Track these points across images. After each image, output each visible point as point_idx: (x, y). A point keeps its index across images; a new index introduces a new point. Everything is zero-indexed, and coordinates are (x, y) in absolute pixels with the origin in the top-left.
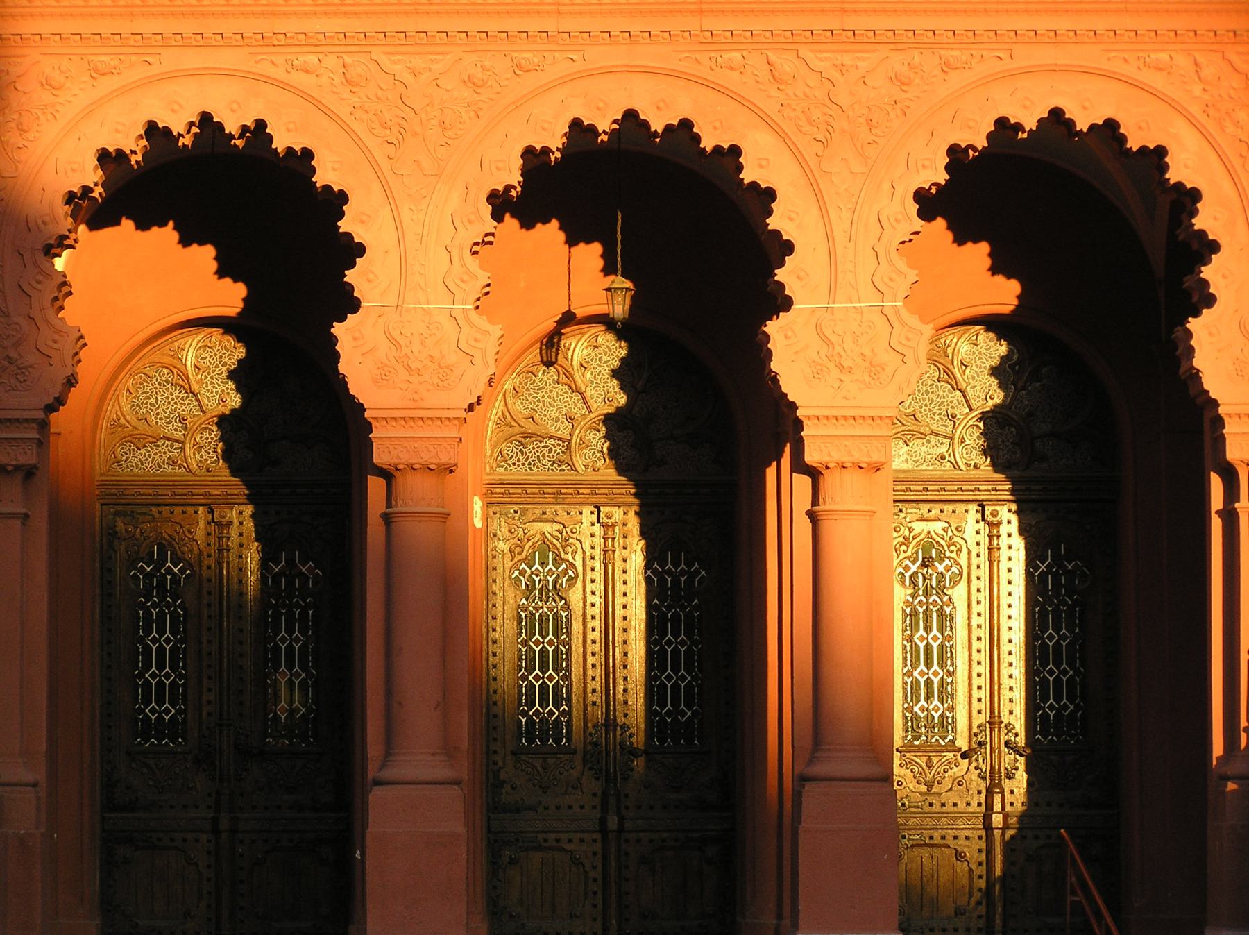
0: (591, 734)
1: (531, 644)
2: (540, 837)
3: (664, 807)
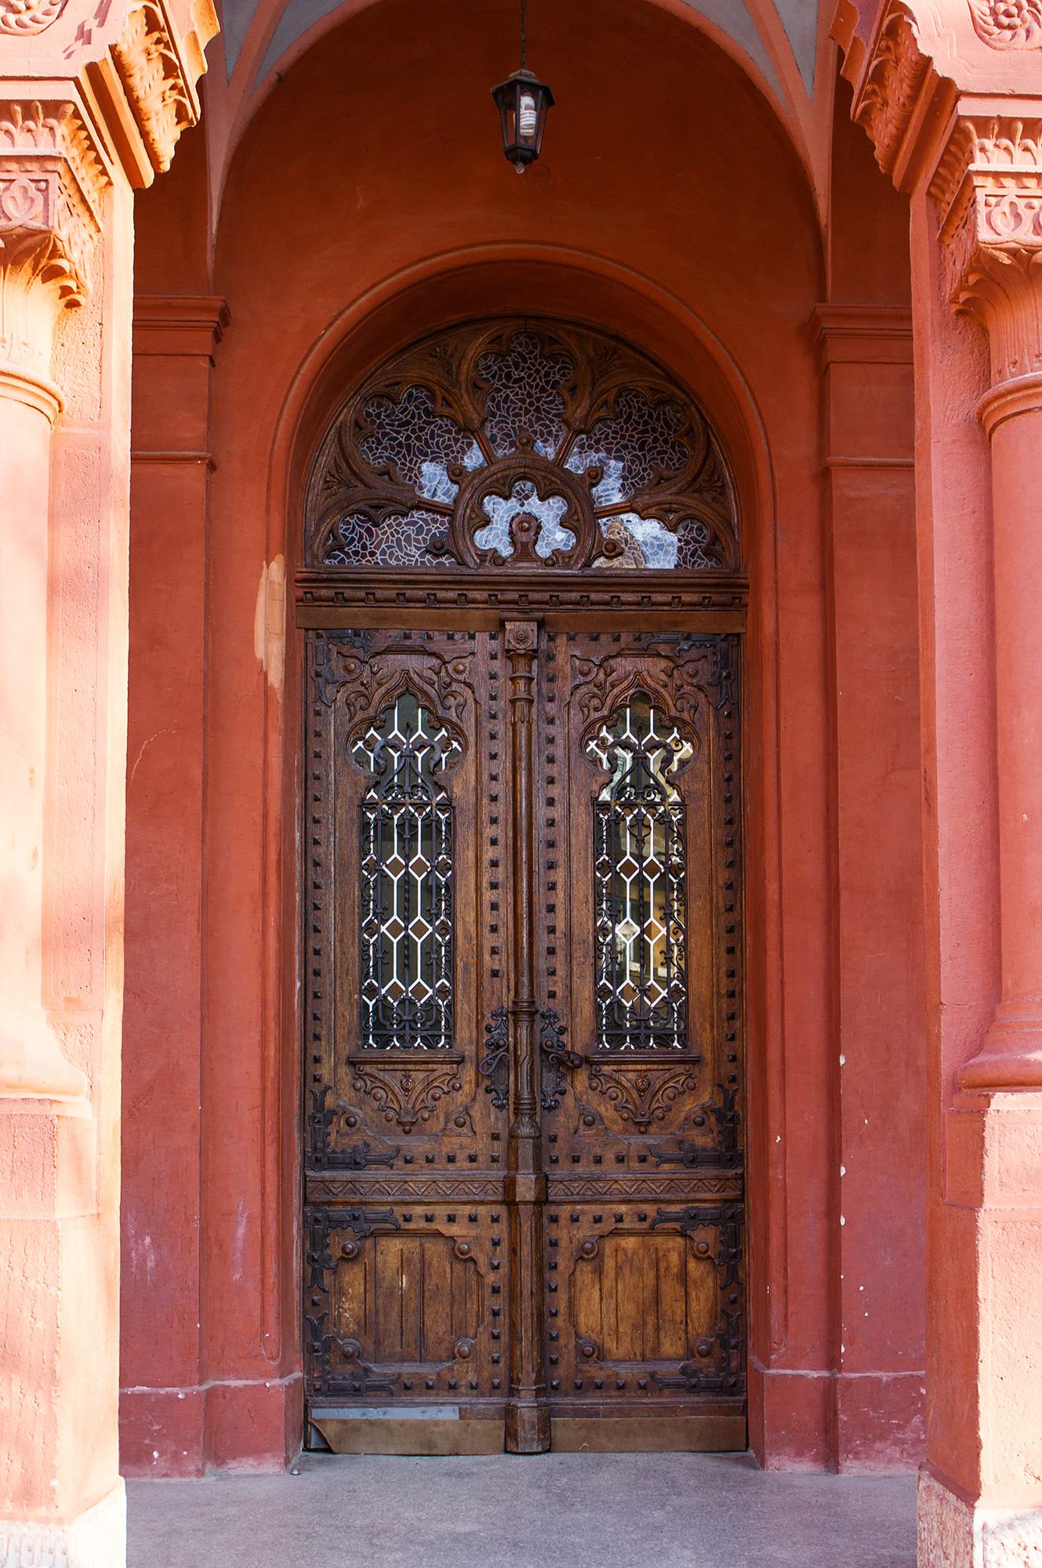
1: (384, 868)
2: (399, 1211)
3: (620, 1159)
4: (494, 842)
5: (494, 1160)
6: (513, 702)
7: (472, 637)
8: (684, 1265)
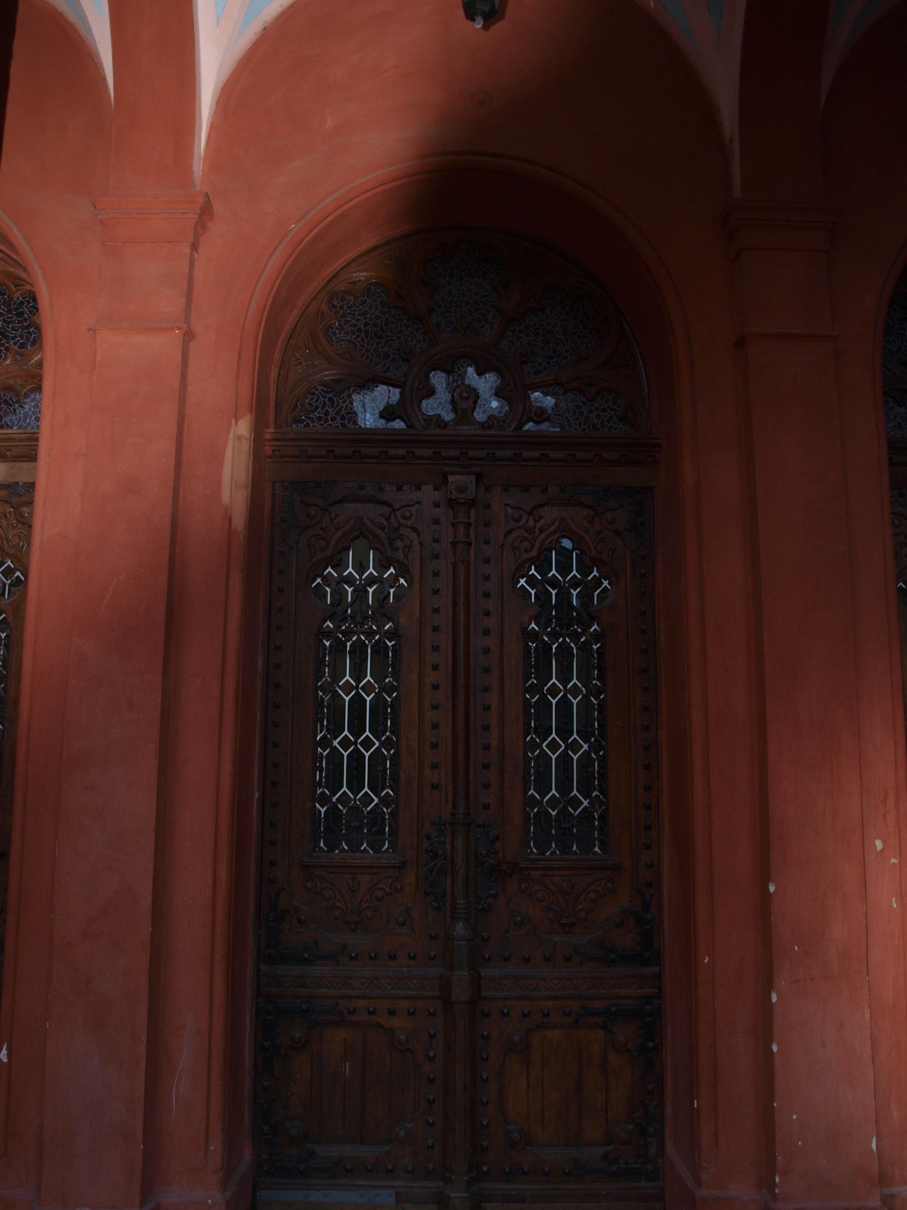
4: (435, 668)
6: (454, 544)
7: (418, 488)
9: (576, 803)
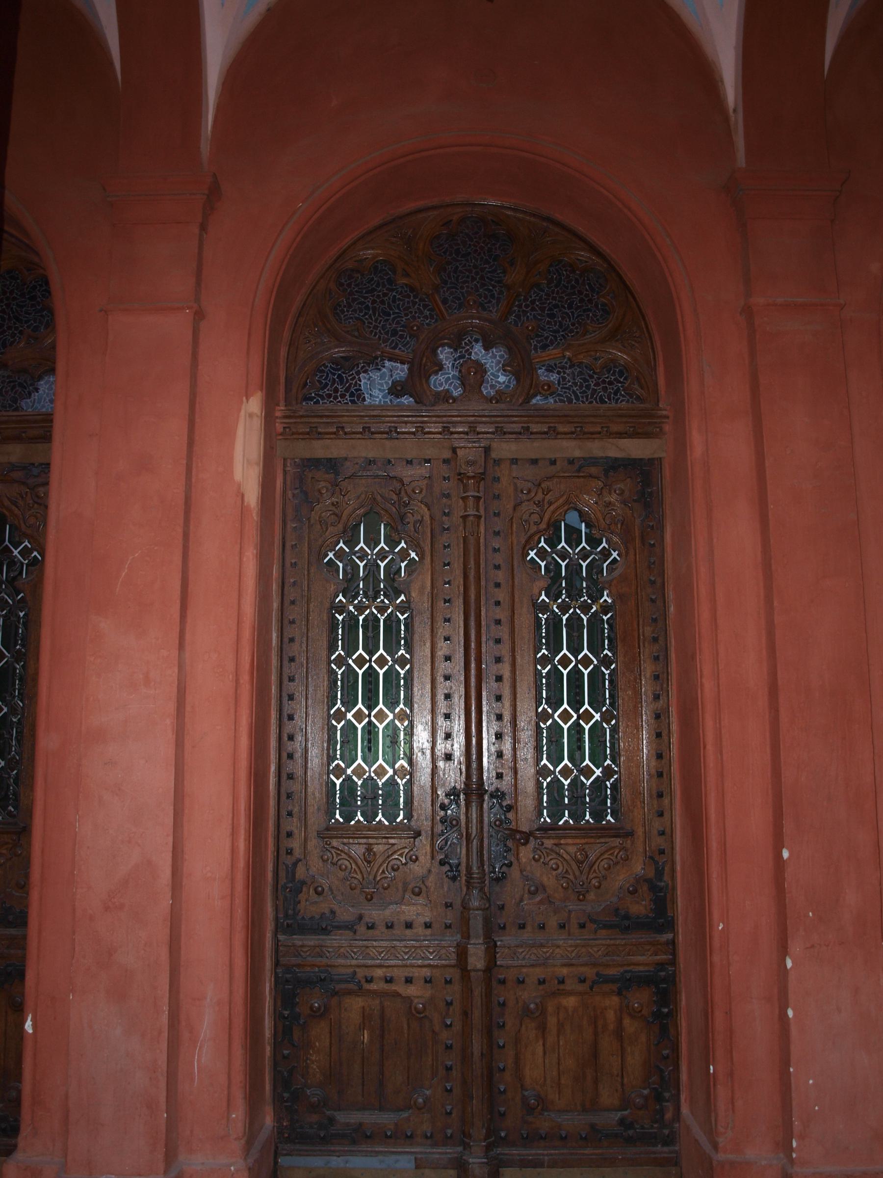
0: (443, 807)
1: (350, 662)
5: (448, 927)
6: (465, 518)
8: (620, 1021)
9: (588, 772)
